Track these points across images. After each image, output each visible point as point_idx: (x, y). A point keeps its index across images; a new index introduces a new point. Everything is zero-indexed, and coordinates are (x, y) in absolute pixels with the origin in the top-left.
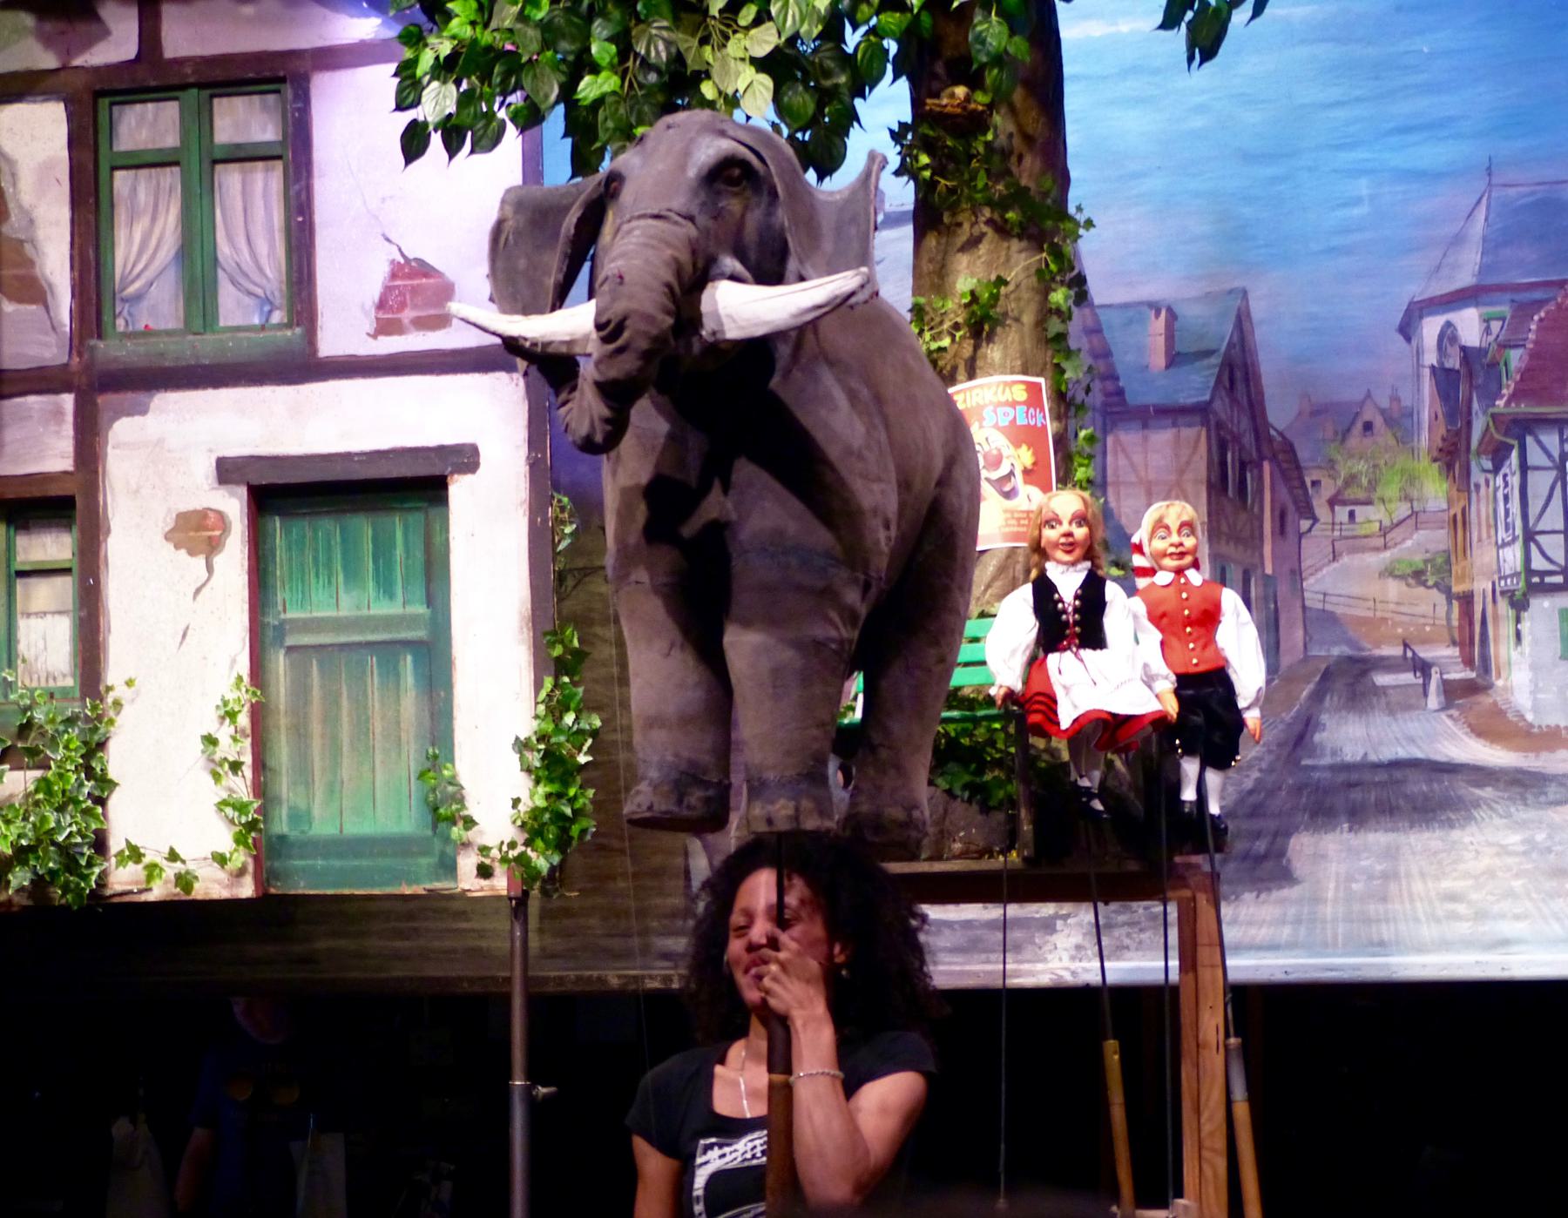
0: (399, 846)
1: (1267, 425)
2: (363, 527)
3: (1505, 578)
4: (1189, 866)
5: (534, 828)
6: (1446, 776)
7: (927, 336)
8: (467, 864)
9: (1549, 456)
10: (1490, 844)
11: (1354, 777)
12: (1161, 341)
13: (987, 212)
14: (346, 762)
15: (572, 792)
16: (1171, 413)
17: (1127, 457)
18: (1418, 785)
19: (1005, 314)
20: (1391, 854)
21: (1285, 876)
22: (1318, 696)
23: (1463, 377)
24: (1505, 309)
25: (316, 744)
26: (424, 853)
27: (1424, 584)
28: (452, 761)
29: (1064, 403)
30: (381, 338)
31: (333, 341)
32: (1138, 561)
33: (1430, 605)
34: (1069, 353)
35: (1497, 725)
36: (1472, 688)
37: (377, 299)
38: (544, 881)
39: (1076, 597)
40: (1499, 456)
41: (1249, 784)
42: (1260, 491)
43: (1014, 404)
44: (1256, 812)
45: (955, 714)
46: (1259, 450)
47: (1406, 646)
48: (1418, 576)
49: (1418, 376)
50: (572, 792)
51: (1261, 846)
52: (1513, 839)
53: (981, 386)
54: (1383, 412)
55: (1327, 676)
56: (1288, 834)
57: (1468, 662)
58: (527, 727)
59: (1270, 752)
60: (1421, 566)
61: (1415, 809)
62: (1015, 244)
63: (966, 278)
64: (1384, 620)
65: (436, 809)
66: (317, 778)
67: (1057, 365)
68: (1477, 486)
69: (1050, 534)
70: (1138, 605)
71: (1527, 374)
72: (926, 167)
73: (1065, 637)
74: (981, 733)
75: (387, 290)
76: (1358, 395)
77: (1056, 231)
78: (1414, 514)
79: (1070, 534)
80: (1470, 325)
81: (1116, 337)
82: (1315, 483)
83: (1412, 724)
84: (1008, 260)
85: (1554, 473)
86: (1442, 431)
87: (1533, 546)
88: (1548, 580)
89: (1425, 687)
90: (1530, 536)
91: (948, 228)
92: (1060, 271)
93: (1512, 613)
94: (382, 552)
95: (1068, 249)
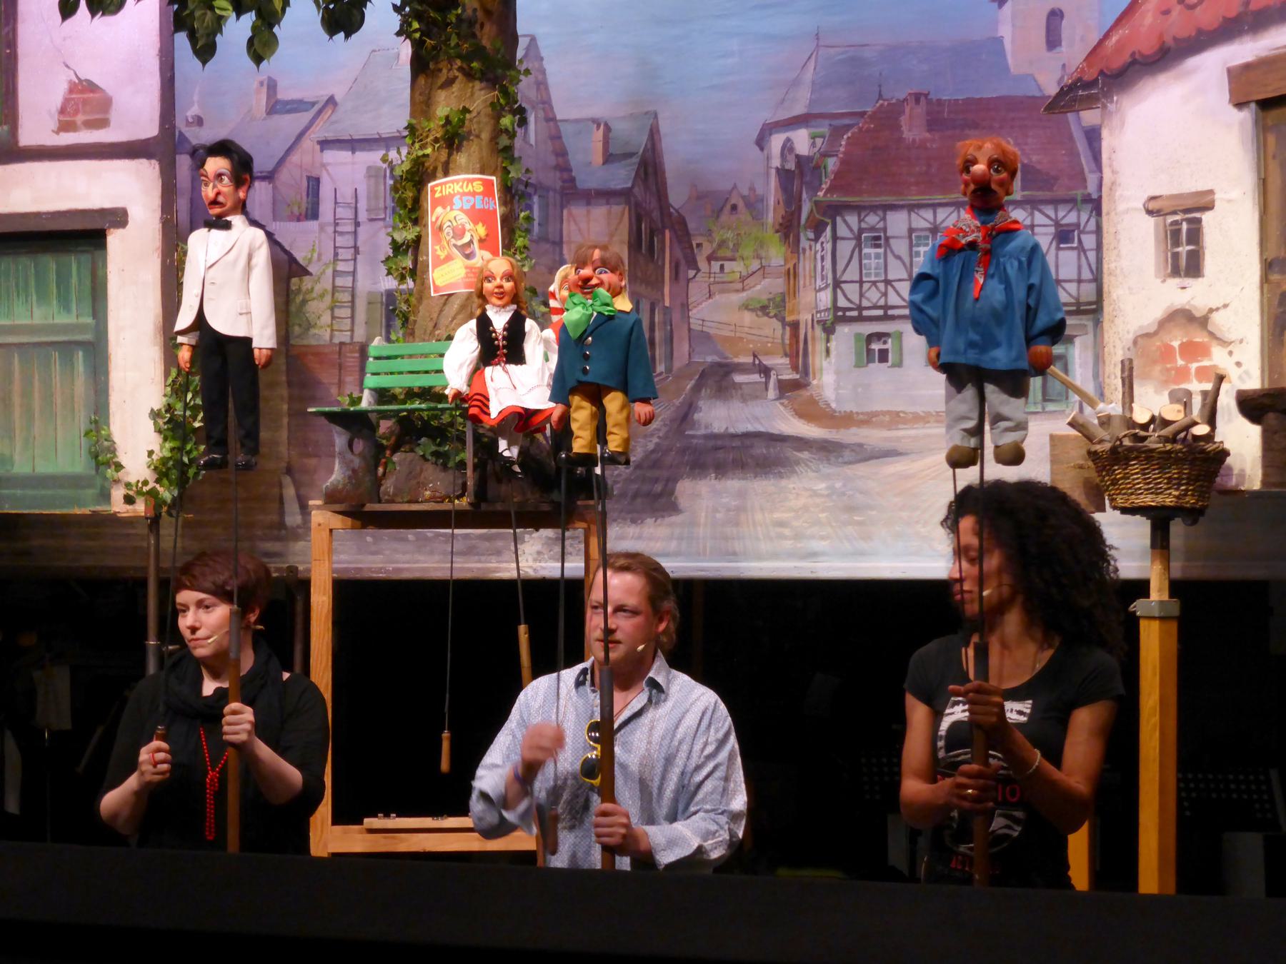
0: (74, 481)
1: (669, 206)
2: (50, 263)
3: (820, 312)
4: (587, 507)
5: (162, 471)
6: (779, 444)
7: (417, 145)
8: (118, 494)
9: (851, 230)
10: (806, 489)
11: (719, 443)
12: (600, 146)
13: (459, 62)
14: (37, 423)
15: (188, 447)
16: (606, 195)
17: (576, 223)
18: (760, 449)
19: (470, 133)
20: (742, 494)
21: (673, 508)
22: (697, 388)
23: (798, 175)
24: (825, 130)
25: (17, 412)
26: (91, 486)
27: (767, 315)
28: (108, 426)
29: (512, 194)
30: (62, 134)
31: (27, 137)
32: (553, 303)
33: (772, 329)
34: (512, 160)
35: (813, 411)
36: (796, 386)
37: (59, 106)
38: (170, 507)
39: (505, 329)
40: (818, 229)
41: (651, 446)
42: (663, 250)
43: (474, 194)
44: (656, 465)
45: (423, 406)
46: (662, 221)
47: (755, 356)
48: (764, 309)
49: (768, 174)
50: (188, 447)
51: (658, 488)
52: (821, 486)
53: (452, 182)
54: (743, 197)
55: (703, 375)
56: (676, 481)
57: (795, 368)
58: (158, 402)
59: (665, 425)
60: (766, 303)
61: (758, 465)
62: (478, 85)
63: (444, 105)
64: (741, 338)
65: (96, 457)
66: (17, 432)
67: (505, 168)
68: (804, 250)
69: (488, 286)
70: (550, 334)
71: (838, 174)
72: (416, 31)
73: (496, 356)
74: (446, 418)
75: (66, 101)
76: (729, 187)
77: (504, 77)
78: (763, 267)
79: (500, 287)
80: (802, 141)
81: (569, 142)
82: (699, 245)
83: (756, 409)
84: (472, 94)
85: (853, 243)
86: (782, 212)
87: (839, 291)
88: (848, 314)
89: (766, 384)
90: (837, 284)
91: (433, 72)
92: (507, 104)
93: (823, 335)
94: (63, 280)
95: (512, 89)
